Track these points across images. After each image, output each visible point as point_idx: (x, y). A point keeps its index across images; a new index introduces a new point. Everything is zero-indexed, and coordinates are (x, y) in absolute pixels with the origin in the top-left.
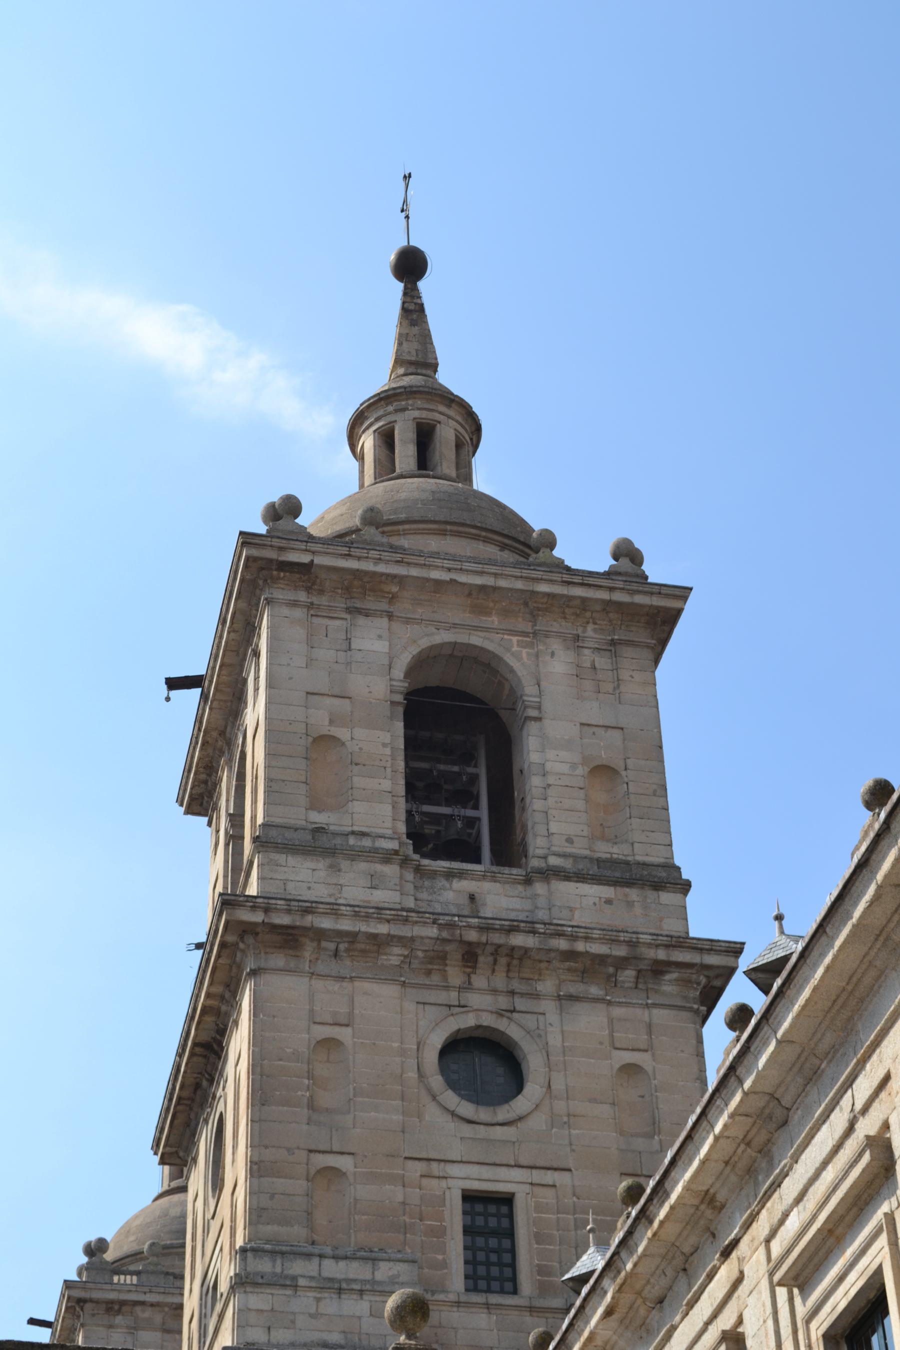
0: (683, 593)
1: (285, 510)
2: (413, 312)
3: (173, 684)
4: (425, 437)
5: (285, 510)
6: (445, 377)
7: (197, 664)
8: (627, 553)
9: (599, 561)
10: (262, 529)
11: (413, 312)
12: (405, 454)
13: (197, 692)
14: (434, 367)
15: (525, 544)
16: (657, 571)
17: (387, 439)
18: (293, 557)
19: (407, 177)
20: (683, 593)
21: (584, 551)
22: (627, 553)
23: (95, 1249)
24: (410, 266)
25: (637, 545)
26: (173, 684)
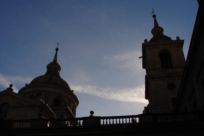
0: (183, 41)
1: (146, 40)
2: (155, 21)
3: (140, 58)
4: (158, 31)
5: (146, 40)
6: (159, 25)
7: (142, 56)
8: (178, 38)
9: (175, 39)
10: (144, 42)
11: (155, 21)
12: (157, 33)
13: (142, 58)
14: (158, 25)
15: (169, 39)
16: (181, 39)
17: (155, 32)
18: (147, 44)
19: (153, 9)
20: (183, 41)
21: (174, 38)
22: (178, 38)
23: (145, 107)
24: (154, 16)
25: (179, 37)
26: (140, 58)
